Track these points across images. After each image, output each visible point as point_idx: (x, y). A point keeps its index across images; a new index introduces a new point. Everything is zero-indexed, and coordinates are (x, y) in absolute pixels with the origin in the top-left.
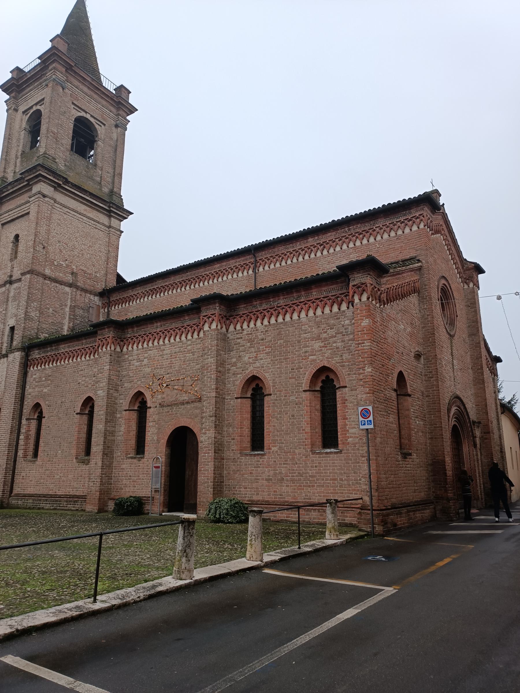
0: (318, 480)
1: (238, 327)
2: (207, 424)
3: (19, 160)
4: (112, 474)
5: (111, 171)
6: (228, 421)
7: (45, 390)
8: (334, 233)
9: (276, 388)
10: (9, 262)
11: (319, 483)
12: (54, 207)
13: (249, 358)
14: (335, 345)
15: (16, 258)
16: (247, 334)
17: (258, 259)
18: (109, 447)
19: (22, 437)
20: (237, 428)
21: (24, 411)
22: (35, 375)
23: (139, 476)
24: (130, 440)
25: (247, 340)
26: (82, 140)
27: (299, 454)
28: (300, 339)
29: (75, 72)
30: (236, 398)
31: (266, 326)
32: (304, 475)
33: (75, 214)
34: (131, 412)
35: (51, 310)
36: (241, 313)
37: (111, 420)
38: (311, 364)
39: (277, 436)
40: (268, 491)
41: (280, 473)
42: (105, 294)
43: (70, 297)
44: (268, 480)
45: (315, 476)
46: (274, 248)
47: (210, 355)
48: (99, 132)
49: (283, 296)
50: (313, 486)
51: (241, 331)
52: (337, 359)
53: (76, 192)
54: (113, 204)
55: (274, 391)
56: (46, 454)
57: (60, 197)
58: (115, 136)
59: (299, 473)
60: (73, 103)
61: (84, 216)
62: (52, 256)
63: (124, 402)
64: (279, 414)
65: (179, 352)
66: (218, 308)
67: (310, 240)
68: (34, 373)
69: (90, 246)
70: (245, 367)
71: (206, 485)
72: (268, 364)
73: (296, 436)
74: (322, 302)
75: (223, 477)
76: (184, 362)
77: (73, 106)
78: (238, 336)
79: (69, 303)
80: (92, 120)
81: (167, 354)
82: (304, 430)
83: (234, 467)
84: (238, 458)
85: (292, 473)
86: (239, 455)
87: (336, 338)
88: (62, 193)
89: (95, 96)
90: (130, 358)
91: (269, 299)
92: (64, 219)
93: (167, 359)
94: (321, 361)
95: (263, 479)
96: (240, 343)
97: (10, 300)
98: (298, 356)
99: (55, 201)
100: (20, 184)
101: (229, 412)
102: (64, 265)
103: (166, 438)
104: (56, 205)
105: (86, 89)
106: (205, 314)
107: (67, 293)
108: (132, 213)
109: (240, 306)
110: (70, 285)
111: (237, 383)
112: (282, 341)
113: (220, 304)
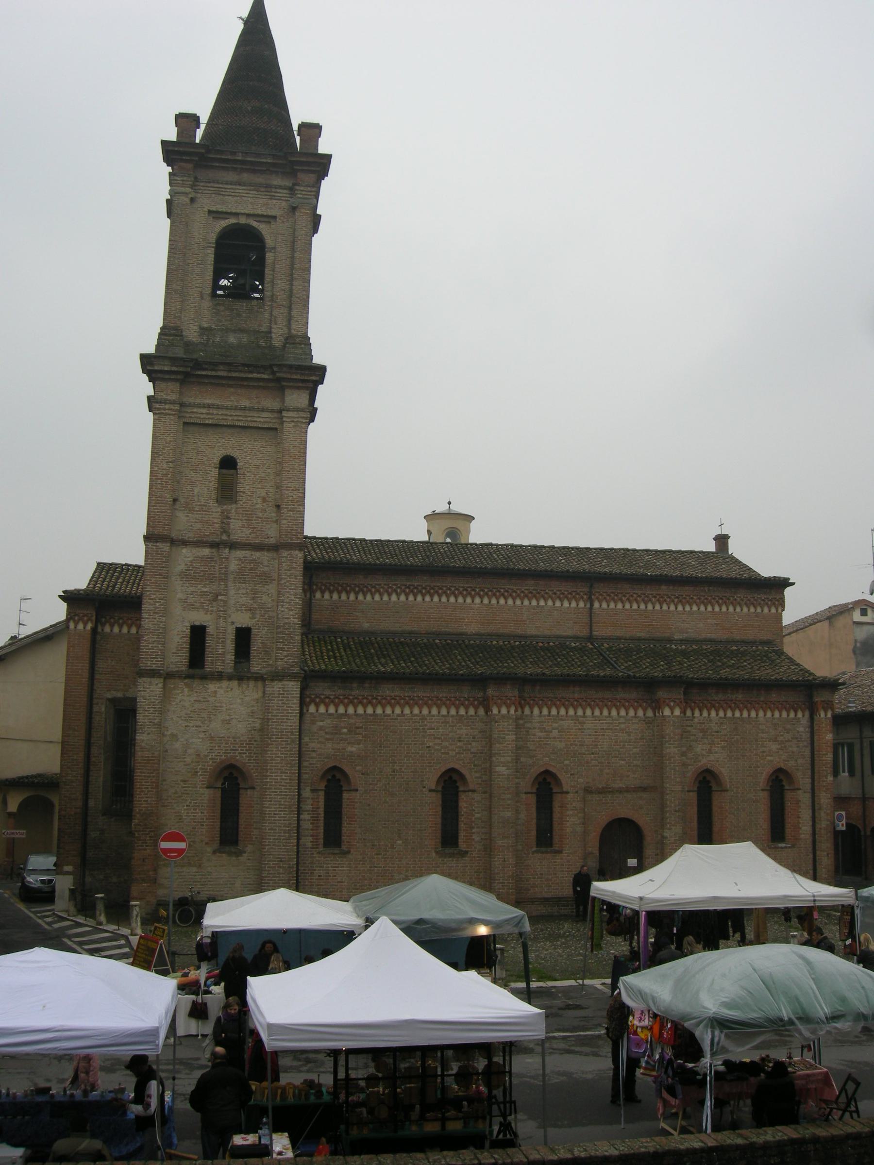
3: (207, 303)
7: (350, 749)
10: (212, 503)
19: (305, 816)
67: (663, 587)
74: (781, 706)
78: (688, 723)
103: (600, 830)
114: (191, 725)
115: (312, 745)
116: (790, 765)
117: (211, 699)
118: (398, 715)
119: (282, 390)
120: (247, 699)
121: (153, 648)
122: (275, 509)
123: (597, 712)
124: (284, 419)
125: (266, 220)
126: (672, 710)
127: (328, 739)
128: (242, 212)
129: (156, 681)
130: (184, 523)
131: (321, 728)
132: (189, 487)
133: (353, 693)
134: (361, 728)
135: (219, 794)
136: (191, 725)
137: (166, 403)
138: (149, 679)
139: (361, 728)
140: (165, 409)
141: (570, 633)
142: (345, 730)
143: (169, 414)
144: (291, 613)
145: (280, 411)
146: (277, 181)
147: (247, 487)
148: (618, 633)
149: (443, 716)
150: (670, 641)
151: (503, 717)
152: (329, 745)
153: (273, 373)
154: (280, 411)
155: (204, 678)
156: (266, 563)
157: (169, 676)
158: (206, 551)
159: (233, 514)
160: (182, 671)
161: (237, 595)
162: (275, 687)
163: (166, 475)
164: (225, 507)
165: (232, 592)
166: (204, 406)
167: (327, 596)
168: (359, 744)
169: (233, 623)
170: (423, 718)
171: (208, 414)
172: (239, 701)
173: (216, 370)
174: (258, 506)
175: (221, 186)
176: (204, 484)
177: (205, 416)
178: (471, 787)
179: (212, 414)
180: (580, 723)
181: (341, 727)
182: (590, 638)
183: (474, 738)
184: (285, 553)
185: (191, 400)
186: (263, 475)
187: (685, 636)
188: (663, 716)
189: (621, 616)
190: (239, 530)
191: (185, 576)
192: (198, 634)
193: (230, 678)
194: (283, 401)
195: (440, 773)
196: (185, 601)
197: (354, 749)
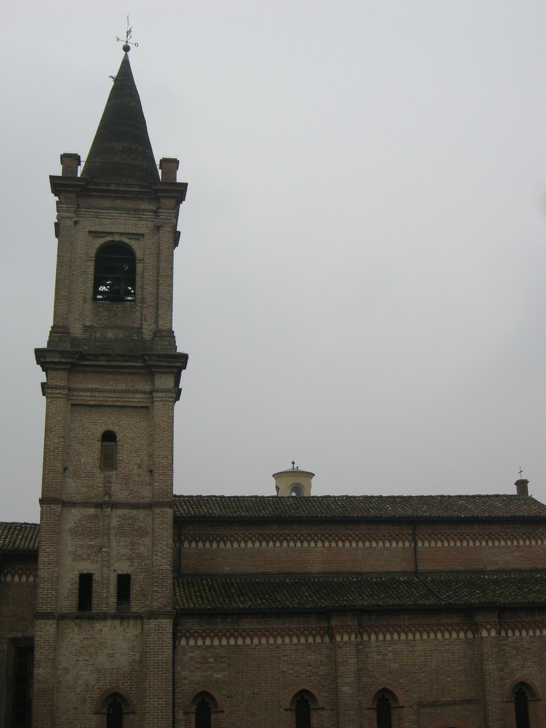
3: (89, 306)
7: (216, 675)
13: (517, 665)
22: (192, 652)
31: (531, 637)
51: (505, 638)
67: (475, 527)
76: (443, 661)
81: (418, 651)
90: (368, 649)
93: (420, 656)
96: (505, 650)
97: (113, 532)
114: (81, 659)
115: (184, 673)
117: (98, 636)
118: (256, 645)
119: (152, 374)
120: (128, 635)
121: (47, 594)
122: (148, 474)
123: (425, 636)
124: (155, 399)
125: (137, 237)
126: (489, 631)
127: (197, 668)
128: (116, 231)
129: (50, 622)
130: (73, 488)
131: (191, 659)
132: (77, 457)
133: (218, 627)
134: (226, 657)
135: (105, 718)
136: (81, 659)
137: (56, 389)
138: (44, 621)
139: (226, 657)
140: (56, 394)
141: (398, 569)
142: (212, 660)
143: (60, 398)
144: (164, 561)
145: (151, 393)
146: (144, 206)
147: (125, 456)
148: (440, 567)
149: (295, 644)
150: (483, 572)
151: (346, 643)
152: (199, 673)
153: (145, 361)
154: (151, 393)
155: (93, 618)
156: (142, 519)
157: (62, 617)
158: (92, 511)
159: (114, 478)
160: (72, 613)
161: (118, 546)
162: (152, 624)
163: (58, 448)
164: (107, 473)
165: (114, 544)
166: (88, 390)
167: (193, 545)
168: (223, 671)
169: (115, 571)
170: (278, 647)
171: (91, 396)
172: (121, 637)
173: (98, 361)
174: (134, 472)
175: (99, 211)
176: (89, 454)
177: (88, 398)
178: (321, 705)
179: (95, 396)
180: (410, 646)
181: (207, 657)
182: (416, 573)
183: (321, 662)
184: (157, 510)
185: (78, 386)
186: (138, 446)
187: (496, 567)
188: (481, 637)
189: (440, 552)
190: (119, 493)
191: (74, 532)
192: (86, 581)
193: (113, 618)
194: (153, 384)
195: (293, 694)
196: (74, 553)
197: (219, 676)
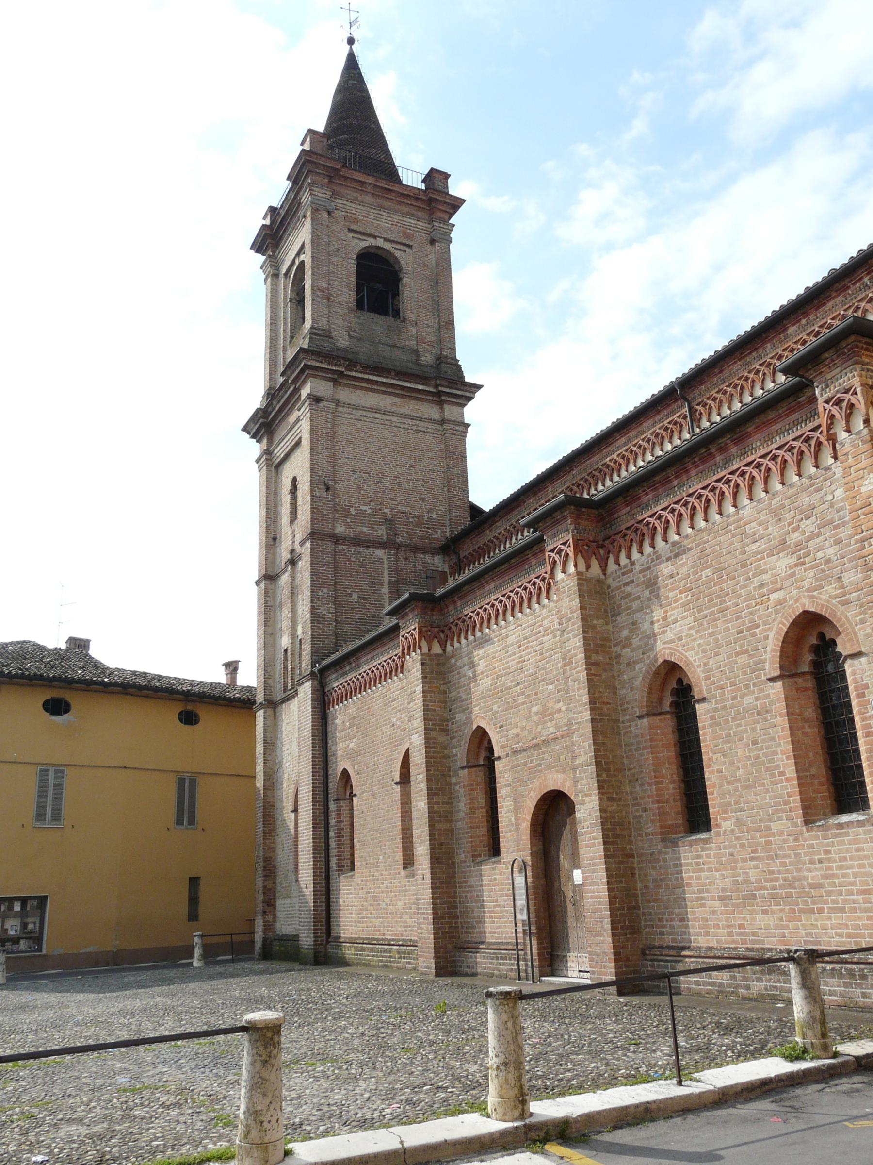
0: (829, 893)
1: (623, 560)
2: (584, 782)
4: (455, 897)
5: (433, 322)
6: (630, 770)
7: (352, 745)
8: (840, 298)
9: (713, 683)
11: (834, 902)
12: (336, 414)
14: (820, 555)
15: (296, 518)
16: (641, 571)
17: (694, 404)
18: (442, 844)
19: (332, 834)
20: (649, 784)
21: (331, 785)
23: (496, 901)
24: (478, 827)
25: (643, 582)
26: (379, 286)
27: (781, 833)
28: (745, 557)
29: (346, 178)
30: (640, 717)
32: (797, 884)
33: (376, 415)
34: (473, 770)
35: (355, 596)
36: (623, 527)
37: (440, 789)
38: (777, 612)
39: (729, 793)
40: (728, 927)
41: (747, 881)
42: (449, 547)
43: (386, 566)
44: (721, 899)
45: (820, 886)
46: (721, 371)
47: (572, 631)
48: (403, 262)
49: (696, 467)
50: (821, 910)
51: (629, 568)
52: (831, 589)
53: (371, 377)
54: (444, 379)
55: (709, 691)
56: (364, 863)
57: (345, 395)
58: (432, 259)
59: (785, 880)
60: (350, 230)
61: (393, 414)
62: (344, 500)
63: (460, 753)
64: (725, 742)
65: (530, 636)
66: (572, 527)
67: (792, 330)
68: (342, 715)
69: (412, 466)
70: (646, 644)
71: (597, 915)
72: (690, 629)
73: (767, 791)
75: (636, 895)
77: (351, 235)
79: (386, 578)
80: (388, 246)
82: (782, 774)
83: (654, 873)
84: (660, 852)
85: (772, 880)
86: (660, 846)
87: (822, 538)
88: (349, 386)
89: (387, 204)
91: (670, 481)
92: (358, 430)
93: (514, 654)
94: (796, 601)
95: (713, 899)
98: (747, 600)
99: (338, 403)
100: (286, 392)
101: (630, 750)
102: (369, 511)
104: (340, 409)
105: (369, 199)
106: (549, 548)
107: (381, 561)
108: (479, 387)
109: (620, 514)
110: (382, 545)
111: (637, 683)
112: (709, 572)
113: (577, 520)
116: (821, 601)
